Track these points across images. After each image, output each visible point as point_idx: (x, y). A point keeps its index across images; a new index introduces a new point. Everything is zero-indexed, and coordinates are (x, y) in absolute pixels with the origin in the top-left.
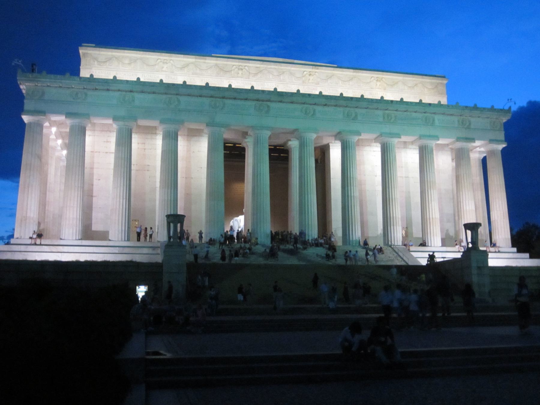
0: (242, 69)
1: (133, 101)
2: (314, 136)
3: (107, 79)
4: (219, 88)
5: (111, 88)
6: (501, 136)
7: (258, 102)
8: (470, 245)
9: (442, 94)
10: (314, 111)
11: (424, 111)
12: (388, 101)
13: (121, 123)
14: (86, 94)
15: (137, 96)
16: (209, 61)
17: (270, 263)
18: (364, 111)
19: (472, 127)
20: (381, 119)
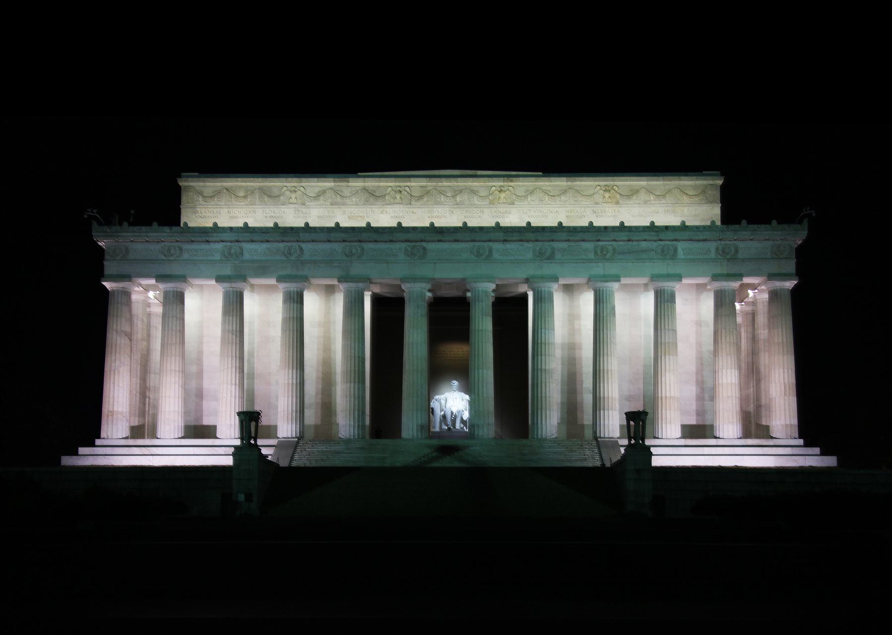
0: (400, 192)
1: (242, 254)
2: (493, 286)
3: (205, 228)
4: (353, 229)
5: (210, 239)
6: (791, 266)
7: (409, 244)
8: (633, 442)
9: (711, 202)
10: (491, 250)
11: (656, 238)
12: (600, 228)
13: (227, 285)
14: (181, 249)
15: (247, 246)
16: (355, 184)
17: (448, 465)
18: (564, 245)
19: (740, 256)
20: (592, 256)
